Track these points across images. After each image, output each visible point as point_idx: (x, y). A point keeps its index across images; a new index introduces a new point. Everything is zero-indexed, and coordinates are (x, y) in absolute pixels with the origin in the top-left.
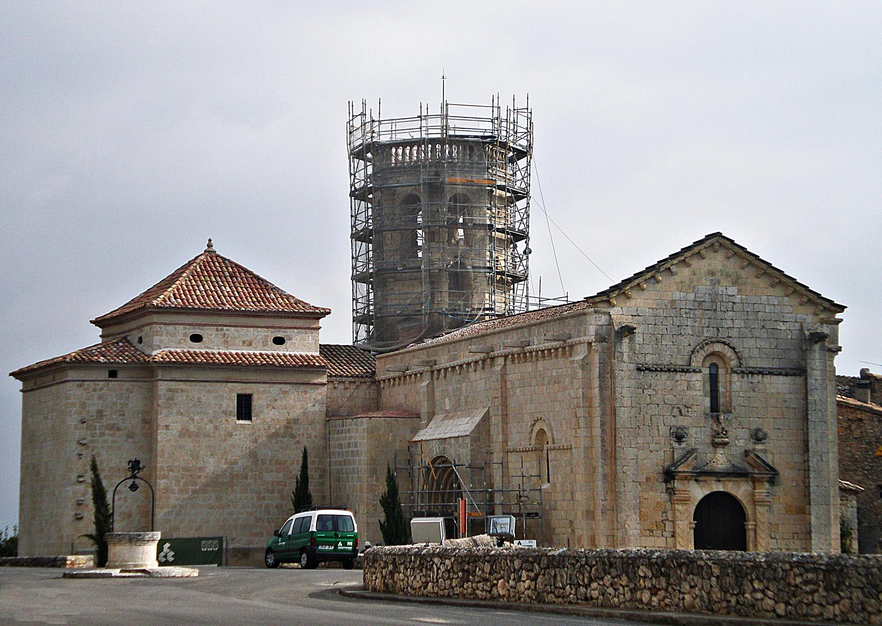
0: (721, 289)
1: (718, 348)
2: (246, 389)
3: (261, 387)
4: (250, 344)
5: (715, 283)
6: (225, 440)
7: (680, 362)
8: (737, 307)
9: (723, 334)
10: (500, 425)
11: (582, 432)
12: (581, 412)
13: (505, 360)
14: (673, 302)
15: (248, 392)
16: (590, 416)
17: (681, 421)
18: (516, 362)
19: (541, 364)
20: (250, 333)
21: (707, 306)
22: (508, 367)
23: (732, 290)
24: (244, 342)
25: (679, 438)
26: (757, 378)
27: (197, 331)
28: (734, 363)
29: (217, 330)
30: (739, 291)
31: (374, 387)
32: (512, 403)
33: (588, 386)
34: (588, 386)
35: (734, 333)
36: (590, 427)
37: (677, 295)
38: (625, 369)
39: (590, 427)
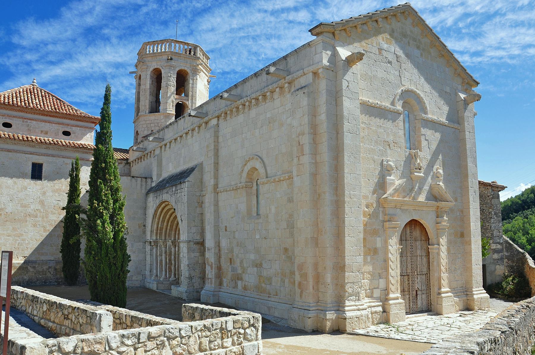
2: (38, 159)
3: (50, 159)
4: (46, 133)
6: (22, 191)
10: (212, 173)
11: (306, 159)
12: (306, 140)
13: (218, 120)
15: (40, 162)
16: (315, 143)
18: (228, 117)
19: (253, 112)
20: (47, 126)
22: (220, 126)
24: (42, 132)
27: (8, 121)
29: (23, 122)
31: (127, 166)
32: (223, 152)
33: (313, 114)
34: (313, 114)
36: (315, 153)
39: (315, 153)
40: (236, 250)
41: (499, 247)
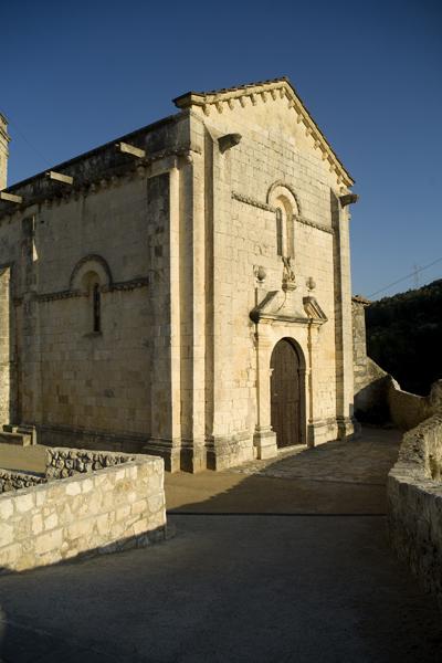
0: (285, 136)
1: (286, 192)
5: (282, 128)
7: (261, 199)
8: (296, 158)
9: (287, 181)
14: (253, 132)
17: (260, 261)
21: (276, 147)
23: (292, 141)
25: (260, 278)
26: (309, 228)
28: (295, 211)
30: (297, 143)
35: (294, 182)
37: (257, 129)
38: (222, 188)
40: (66, 376)
41: (362, 369)
